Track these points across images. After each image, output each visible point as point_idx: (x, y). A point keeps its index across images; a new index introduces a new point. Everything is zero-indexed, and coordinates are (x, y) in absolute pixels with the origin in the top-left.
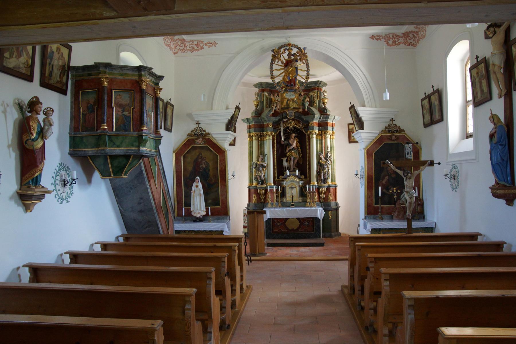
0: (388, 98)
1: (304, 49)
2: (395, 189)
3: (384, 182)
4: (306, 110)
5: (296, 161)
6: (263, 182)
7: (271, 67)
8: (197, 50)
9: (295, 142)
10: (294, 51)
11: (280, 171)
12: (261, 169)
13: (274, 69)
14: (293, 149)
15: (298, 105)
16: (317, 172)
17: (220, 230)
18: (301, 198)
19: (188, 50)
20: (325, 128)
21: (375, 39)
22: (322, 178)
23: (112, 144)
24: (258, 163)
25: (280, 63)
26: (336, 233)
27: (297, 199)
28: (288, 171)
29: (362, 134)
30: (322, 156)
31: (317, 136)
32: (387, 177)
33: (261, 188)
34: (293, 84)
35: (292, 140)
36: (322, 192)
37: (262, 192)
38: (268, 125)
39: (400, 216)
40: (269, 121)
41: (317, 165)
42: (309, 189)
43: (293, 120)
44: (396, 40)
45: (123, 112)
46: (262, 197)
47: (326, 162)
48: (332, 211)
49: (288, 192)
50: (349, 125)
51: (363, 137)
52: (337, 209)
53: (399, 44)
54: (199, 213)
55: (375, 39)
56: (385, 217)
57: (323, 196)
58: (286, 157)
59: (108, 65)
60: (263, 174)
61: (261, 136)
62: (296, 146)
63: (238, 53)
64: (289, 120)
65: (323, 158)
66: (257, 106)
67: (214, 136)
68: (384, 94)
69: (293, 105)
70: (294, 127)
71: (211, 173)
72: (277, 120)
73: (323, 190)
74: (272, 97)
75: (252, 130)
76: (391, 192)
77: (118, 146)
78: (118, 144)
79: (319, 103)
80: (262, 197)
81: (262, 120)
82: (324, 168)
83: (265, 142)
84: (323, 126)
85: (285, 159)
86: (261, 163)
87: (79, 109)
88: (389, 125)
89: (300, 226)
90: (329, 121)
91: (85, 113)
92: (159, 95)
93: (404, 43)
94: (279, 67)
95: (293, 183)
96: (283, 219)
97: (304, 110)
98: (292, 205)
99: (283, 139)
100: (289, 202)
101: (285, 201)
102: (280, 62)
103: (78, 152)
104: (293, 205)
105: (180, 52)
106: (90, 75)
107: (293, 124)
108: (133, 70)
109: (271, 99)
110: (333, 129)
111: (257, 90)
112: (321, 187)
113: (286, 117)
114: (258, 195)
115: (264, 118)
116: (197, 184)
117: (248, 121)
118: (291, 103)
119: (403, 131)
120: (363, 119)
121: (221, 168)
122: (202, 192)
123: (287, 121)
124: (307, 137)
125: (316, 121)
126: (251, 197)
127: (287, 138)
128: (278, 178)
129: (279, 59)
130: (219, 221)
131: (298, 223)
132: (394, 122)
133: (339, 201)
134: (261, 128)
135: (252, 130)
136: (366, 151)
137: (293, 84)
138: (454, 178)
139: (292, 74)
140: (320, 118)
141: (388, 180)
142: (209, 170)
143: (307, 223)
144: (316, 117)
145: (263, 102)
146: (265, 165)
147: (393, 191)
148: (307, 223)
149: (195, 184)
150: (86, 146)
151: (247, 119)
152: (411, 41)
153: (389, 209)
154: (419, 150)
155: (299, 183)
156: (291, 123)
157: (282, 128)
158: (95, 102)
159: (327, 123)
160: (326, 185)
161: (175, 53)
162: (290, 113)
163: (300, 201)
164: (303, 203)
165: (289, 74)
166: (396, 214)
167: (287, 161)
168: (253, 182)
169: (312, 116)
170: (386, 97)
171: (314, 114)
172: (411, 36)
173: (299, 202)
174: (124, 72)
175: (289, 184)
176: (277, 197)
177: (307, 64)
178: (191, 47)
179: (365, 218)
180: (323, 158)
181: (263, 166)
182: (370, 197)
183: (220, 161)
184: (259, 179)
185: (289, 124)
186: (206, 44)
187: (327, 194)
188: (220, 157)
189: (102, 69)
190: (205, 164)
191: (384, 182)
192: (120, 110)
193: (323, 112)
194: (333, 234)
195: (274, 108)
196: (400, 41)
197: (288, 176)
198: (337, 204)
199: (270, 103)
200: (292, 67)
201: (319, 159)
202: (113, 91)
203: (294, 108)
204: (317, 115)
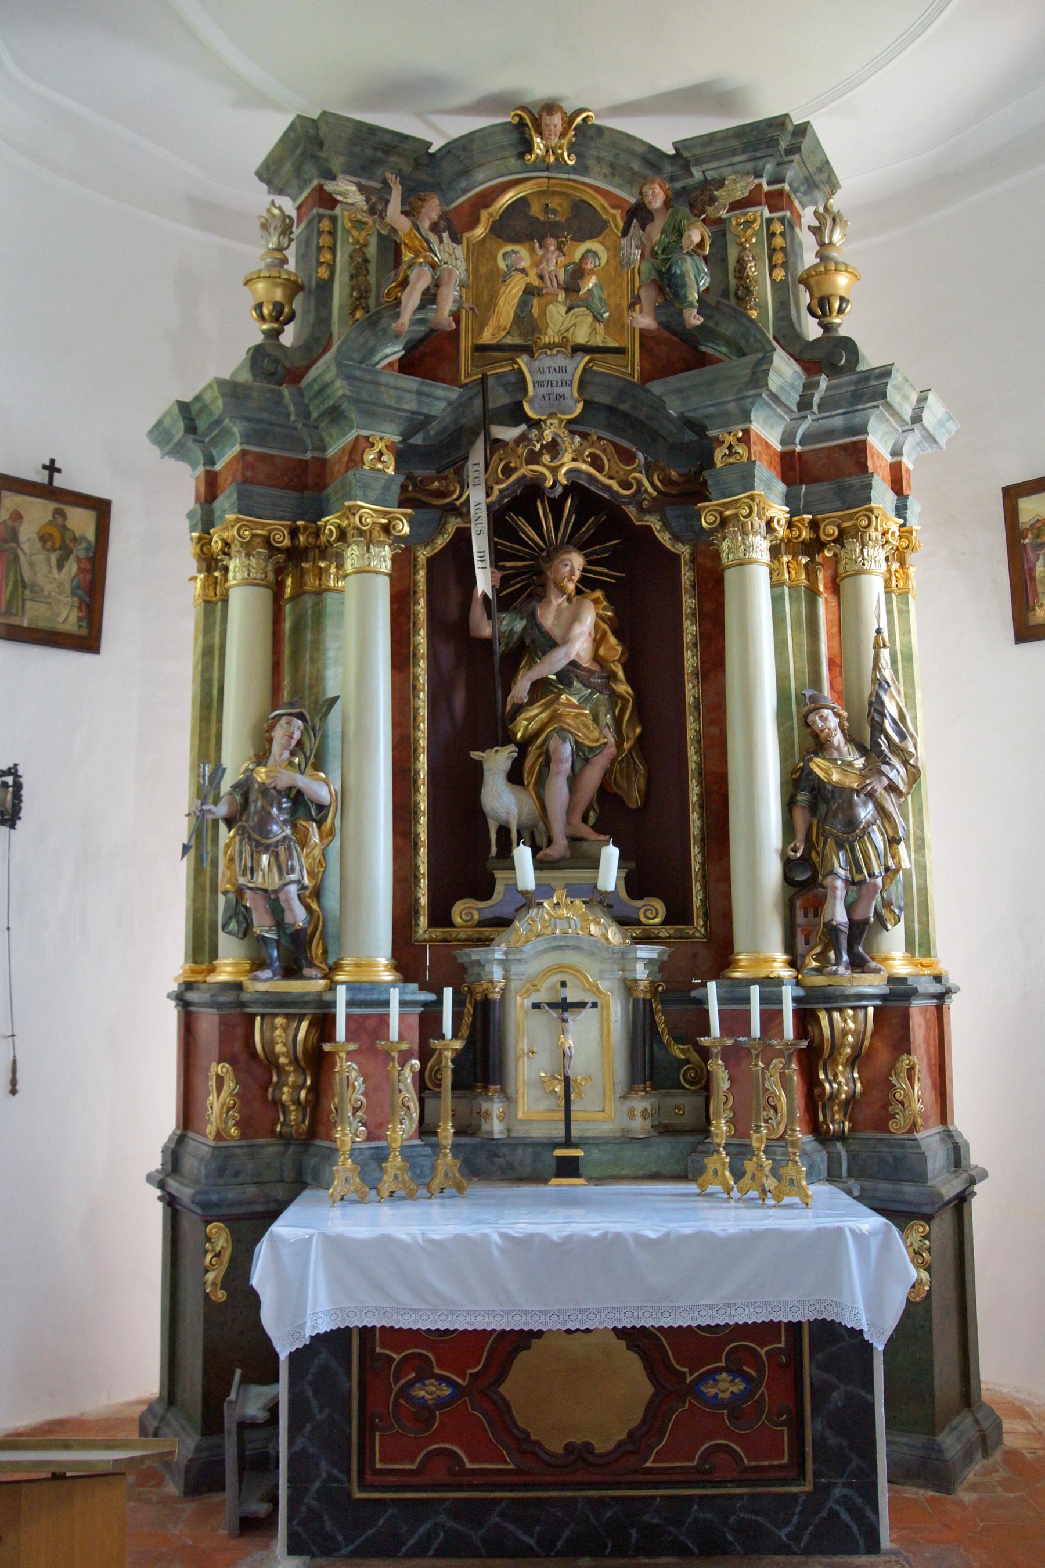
5: (593, 777)
6: (297, 950)
11: (456, 860)
12: (278, 830)
16: (788, 865)
18: (640, 1103)
27: (608, 1108)
28: (523, 854)
30: (830, 722)
31: (775, 552)
33: (279, 1002)
35: (557, 601)
37: (283, 1038)
38: (354, 454)
41: (789, 805)
42: (735, 1021)
46: (291, 1089)
49: (530, 1049)
50: (1012, 495)
52: (962, 1201)
57: (842, 1081)
58: (507, 739)
60: (300, 873)
61: (295, 555)
62: (596, 658)
65: (838, 738)
66: (281, 316)
73: (847, 1025)
75: (226, 505)
80: (291, 1089)
82: (852, 822)
83: (331, 601)
84: (831, 479)
85: (497, 762)
89: (655, 1414)
90: (879, 441)
95: (568, 966)
96: (479, 1336)
99: (484, 582)
100: (537, 1133)
101: (497, 1128)
104: (568, 1168)
107: (567, 463)
112: (832, 999)
113: (515, 415)
114: (254, 1068)
117: (191, 429)
123: (523, 438)
124: (687, 575)
125: (768, 430)
128: (440, 917)
131: (633, 1382)
133: (962, 1120)
134: (301, 488)
135: (226, 505)
143: (726, 1387)
145: (325, 287)
148: (726, 1387)
151: (184, 407)
155: (623, 958)
156: (554, 448)
157: (477, 498)
159: (858, 452)
160: (871, 984)
162: (552, 384)
164: (664, 1148)
167: (515, 776)
168: (214, 955)
173: (627, 1139)
175: (534, 967)
176: (424, 1086)
180: (838, 738)
184: (262, 924)
185: (534, 458)
187: (883, 1056)
194: (950, 1442)
201: (804, 742)
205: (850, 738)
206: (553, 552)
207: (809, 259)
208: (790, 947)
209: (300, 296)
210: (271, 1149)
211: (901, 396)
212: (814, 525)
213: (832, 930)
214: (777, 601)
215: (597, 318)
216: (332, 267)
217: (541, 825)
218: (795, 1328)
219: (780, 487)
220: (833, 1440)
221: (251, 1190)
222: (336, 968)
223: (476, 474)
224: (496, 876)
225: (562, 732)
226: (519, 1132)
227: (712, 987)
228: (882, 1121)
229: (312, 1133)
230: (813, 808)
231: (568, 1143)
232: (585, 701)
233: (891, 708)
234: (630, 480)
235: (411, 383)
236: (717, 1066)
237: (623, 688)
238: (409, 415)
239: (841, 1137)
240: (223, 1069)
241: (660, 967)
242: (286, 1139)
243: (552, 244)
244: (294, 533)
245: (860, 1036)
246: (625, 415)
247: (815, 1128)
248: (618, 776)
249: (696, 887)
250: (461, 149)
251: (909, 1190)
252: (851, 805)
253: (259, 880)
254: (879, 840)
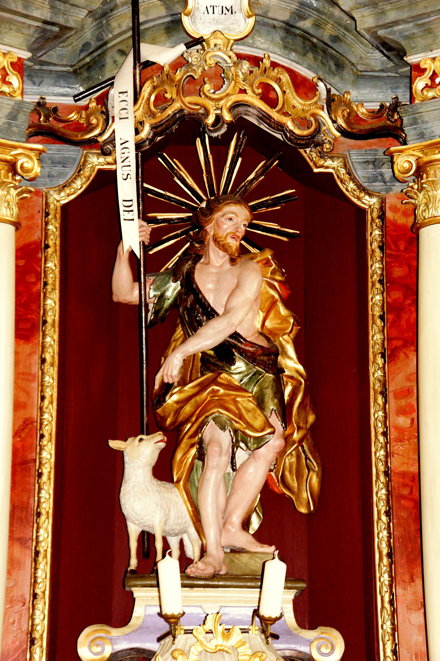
14: (224, 354)
58: (155, 425)
85: (140, 453)
99: (133, 234)
167: (163, 470)
217: (192, 530)
223: (123, 105)
224: (135, 595)
238: (39, 24)
246: (305, 36)
248: (287, 474)
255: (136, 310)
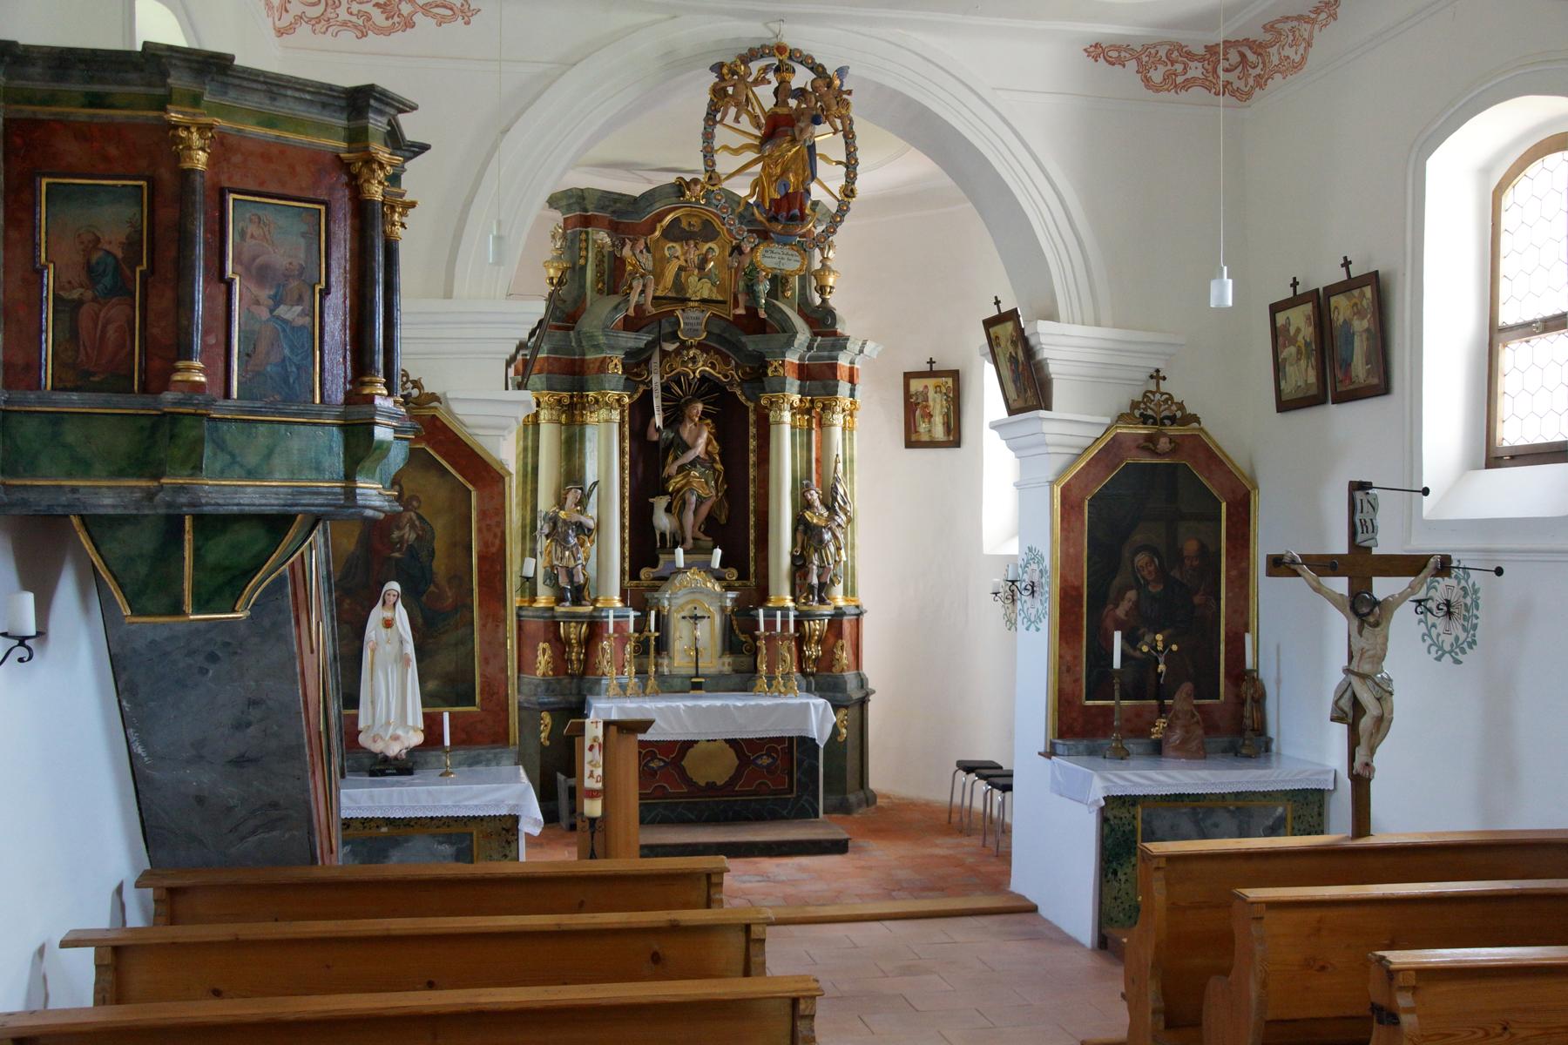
0: (1230, 303)
1: (841, 72)
2: (1159, 637)
3: (1121, 612)
4: (762, 314)
5: (705, 510)
7: (708, 136)
8: (386, 32)
9: (705, 435)
10: (801, 78)
12: (573, 541)
13: (717, 144)
14: (693, 463)
15: (721, 289)
16: (793, 557)
17: (504, 812)
18: (727, 659)
19: (345, 24)
20: (825, 387)
21: (1101, 60)
22: (815, 581)
23: (223, 459)
24: (562, 514)
25: (745, 123)
26: (861, 794)
27: (714, 662)
29: (1047, 427)
30: (814, 496)
31: (793, 415)
32: (1131, 595)
33: (573, 616)
34: (797, 211)
35: (690, 425)
36: (811, 636)
37: (575, 632)
39: (1194, 745)
40: (612, 348)
41: (795, 531)
42: (770, 625)
43: (702, 346)
44: (1179, 67)
45: (277, 305)
47: (831, 518)
48: (853, 706)
50: (908, 376)
51: (1049, 439)
52: (863, 703)
53: (1187, 85)
54: (396, 738)
55: (1101, 60)
56: (1131, 745)
57: (813, 651)
58: (665, 492)
59: (214, 66)
62: (707, 452)
63: (568, 64)
64: (684, 346)
65: (817, 503)
66: (560, 282)
67: (458, 409)
68: (1214, 284)
69: (700, 289)
70: (704, 378)
71: (440, 566)
72: (642, 345)
73: (816, 627)
74: (627, 252)
76: (1145, 649)
77: (251, 474)
78: (252, 459)
79: (803, 288)
81: (579, 342)
82: (821, 541)
84: (820, 380)
85: (661, 503)
86: (576, 517)
87: (39, 273)
88: (1145, 395)
89: (739, 769)
90: (843, 361)
91: (75, 295)
92: (399, 230)
93: (1208, 84)
94: (738, 141)
95: (696, 600)
97: (752, 311)
98: (695, 685)
99: (658, 420)
100: (683, 672)
101: (666, 670)
102: (744, 118)
103: (32, 497)
104: (697, 687)
105: (304, 29)
106: (95, 101)
107: (702, 367)
108: (324, 106)
109: (622, 261)
110: (852, 395)
111: (558, 217)
113: (673, 337)
115: (591, 337)
116: (388, 614)
118: (693, 279)
119: (1195, 419)
120: (1053, 369)
121: (485, 544)
122: (410, 649)
123: (677, 352)
124: (752, 417)
125: (792, 358)
126: (527, 651)
127: (675, 417)
129: (744, 105)
130: (480, 768)
131: (731, 759)
132: (1164, 386)
133: (867, 669)
134: (573, 373)
136: (1057, 491)
137: (797, 211)
138: (1449, 614)
139: (796, 174)
140: (810, 348)
141: (1137, 605)
142: (432, 554)
144: (796, 343)
145: (583, 268)
146: (592, 524)
147: (1154, 648)
148: (765, 761)
149: (377, 614)
150: (82, 466)
152: (1232, 77)
153: (1138, 715)
154: (1248, 495)
155: (721, 597)
156: (694, 360)
157: (656, 380)
158: (132, 245)
159: (833, 368)
160: (827, 610)
161: (280, 32)
162: (691, 320)
163: (727, 669)
164: (736, 679)
165: (784, 172)
166: (1176, 736)
167: (668, 510)
169: (783, 337)
170: (1222, 296)
171: (789, 332)
172: (1234, 57)
173: (721, 675)
174: (283, 108)
175: (681, 601)
177: (849, 137)
178: (359, 14)
179: (1050, 753)
180: (817, 503)
181: (580, 528)
182: (1068, 670)
183: (483, 515)
184: (563, 581)
185: (684, 363)
186: (426, 9)
187: (831, 640)
188: (481, 499)
189: (179, 80)
190: (413, 526)
191: (1121, 612)
192: (264, 294)
193: (822, 321)
194: (852, 798)
195: (634, 298)
196: (1190, 74)
197: (679, 571)
198: (862, 682)
199: (615, 276)
200: (794, 141)
201: (802, 504)
202: (231, 197)
203: (703, 301)
204: (803, 335)
205: (823, 502)
206: (689, 403)
207: (817, 265)
208: (793, 593)
209: (572, 273)
210: (566, 681)
211: (853, 346)
212: (812, 401)
213: (811, 587)
214: (793, 435)
215: (714, 284)
216: (586, 258)
218: (791, 739)
219: (798, 382)
220: (804, 779)
221: (561, 698)
222: (596, 600)
225: (692, 490)
226: (675, 672)
227: (761, 611)
228: (830, 667)
229: (584, 673)
230: (805, 532)
231: (697, 676)
232: (702, 474)
233: (841, 491)
234: (727, 373)
235: (632, 335)
236: (762, 643)
237: (719, 466)
239: (812, 674)
240: (546, 645)
241: (735, 600)
242: (572, 676)
243: (692, 243)
244: (572, 397)
245: (821, 631)
247: (801, 670)
249: (752, 564)
250: (649, 197)
251: (839, 695)
252: (821, 534)
253: (565, 563)
254: (832, 549)
255: (656, 443)
